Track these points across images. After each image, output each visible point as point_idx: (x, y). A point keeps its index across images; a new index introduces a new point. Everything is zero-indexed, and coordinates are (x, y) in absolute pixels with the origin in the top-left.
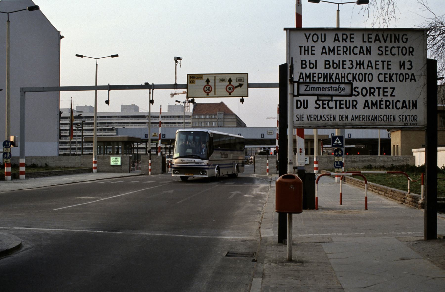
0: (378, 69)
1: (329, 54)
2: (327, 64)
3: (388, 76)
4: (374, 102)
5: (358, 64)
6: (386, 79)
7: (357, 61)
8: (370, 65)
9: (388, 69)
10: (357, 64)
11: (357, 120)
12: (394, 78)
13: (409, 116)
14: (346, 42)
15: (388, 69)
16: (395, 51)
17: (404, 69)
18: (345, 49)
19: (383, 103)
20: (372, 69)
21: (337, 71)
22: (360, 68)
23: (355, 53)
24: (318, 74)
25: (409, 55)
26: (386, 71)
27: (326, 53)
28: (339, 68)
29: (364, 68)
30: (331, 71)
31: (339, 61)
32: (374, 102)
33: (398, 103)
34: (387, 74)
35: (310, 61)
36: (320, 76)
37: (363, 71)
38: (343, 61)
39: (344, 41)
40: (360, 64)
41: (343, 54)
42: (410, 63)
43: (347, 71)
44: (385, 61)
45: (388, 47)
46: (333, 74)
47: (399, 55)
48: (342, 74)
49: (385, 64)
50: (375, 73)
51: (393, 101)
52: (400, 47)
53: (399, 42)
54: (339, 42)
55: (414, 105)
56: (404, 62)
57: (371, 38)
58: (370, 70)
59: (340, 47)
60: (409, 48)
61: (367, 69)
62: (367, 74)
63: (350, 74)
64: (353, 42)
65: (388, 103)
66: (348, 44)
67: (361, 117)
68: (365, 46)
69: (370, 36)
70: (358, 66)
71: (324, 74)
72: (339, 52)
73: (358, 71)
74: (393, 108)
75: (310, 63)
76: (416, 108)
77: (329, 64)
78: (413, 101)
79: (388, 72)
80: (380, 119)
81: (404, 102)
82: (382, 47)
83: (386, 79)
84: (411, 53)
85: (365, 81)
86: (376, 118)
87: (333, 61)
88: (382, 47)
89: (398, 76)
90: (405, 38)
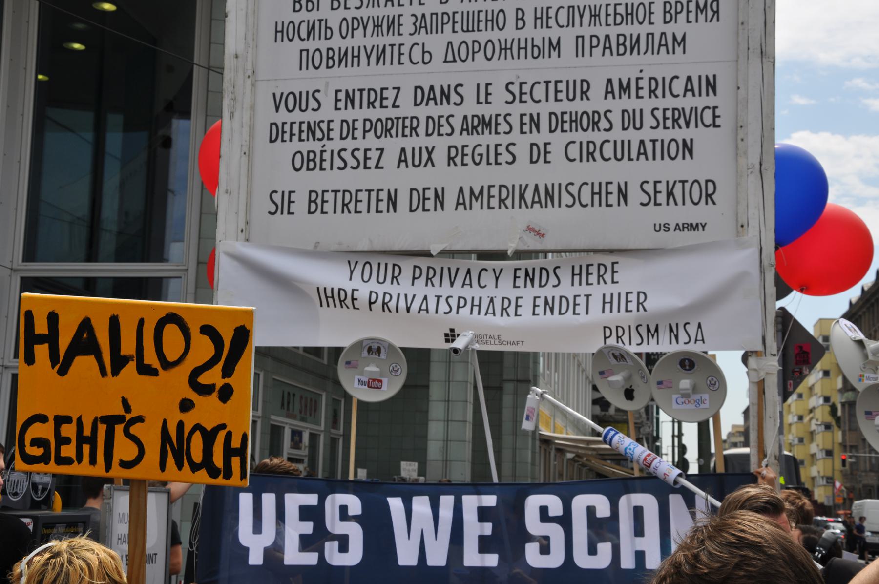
11: (476, 205)
13: (683, 182)
67: (494, 191)
80: (567, 199)
86: (549, 195)
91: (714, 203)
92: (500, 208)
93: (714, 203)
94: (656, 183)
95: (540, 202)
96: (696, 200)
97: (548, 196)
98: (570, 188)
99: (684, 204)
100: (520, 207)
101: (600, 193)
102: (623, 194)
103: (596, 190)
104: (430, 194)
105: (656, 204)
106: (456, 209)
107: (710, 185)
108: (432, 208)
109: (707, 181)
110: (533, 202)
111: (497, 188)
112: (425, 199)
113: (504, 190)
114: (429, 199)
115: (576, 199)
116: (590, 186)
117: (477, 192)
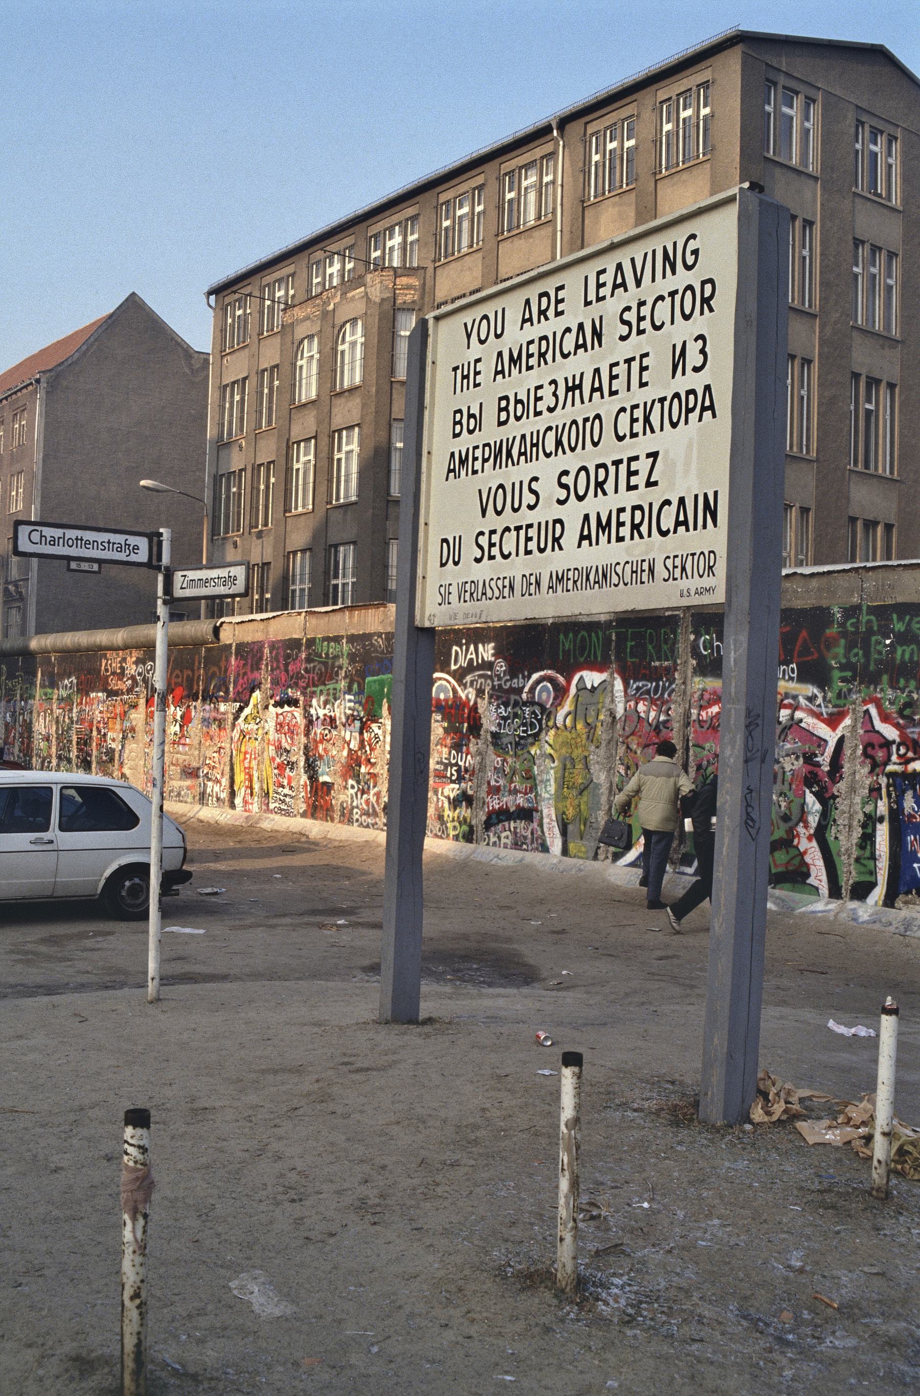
3: (639, 413)
10: (568, 389)
13: (693, 555)
16: (663, 311)
19: (626, 517)
29: (582, 402)
30: (514, 429)
44: (633, 359)
80: (615, 580)
86: (605, 576)
101: (636, 572)
102: (651, 571)
110: (595, 582)
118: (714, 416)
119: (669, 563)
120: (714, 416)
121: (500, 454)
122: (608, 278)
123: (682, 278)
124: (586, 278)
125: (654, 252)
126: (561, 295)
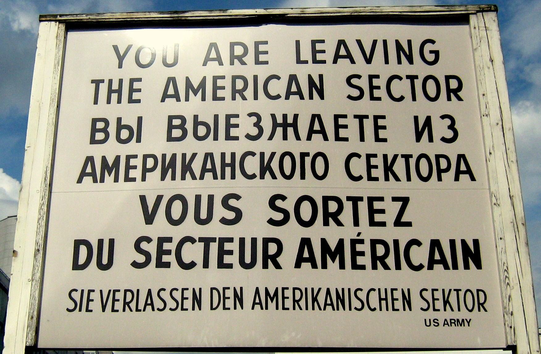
0: (346, 139)
1: (187, 99)
2: (176, 127)
3: (378, 161)
4: (333, 246)
5: (280, 125)
6: (374, 173)
7: (273, 116)
8: (317, 127)
9: (378, 139)
10: (275, 125)
11: (272, 305)
12: (399, 167)
13: (458, 291)
14: (243, 63)
15: (378, 139)
16: (401, 88)
17: (431, 140)
18: (240, 84)
19: (366, 248)
20: (326, 138)
21: (209, 146)
22: (285, 137)
23: (273, 93)
24: (145, 157)
25: (449, 99)
26: (370, 145)
27: (176, 96)
28: (216, 138)
30: (189, 146)
31: (216, 117)
32: (333, 246)
33: (414, 248)
34: (375, 156)
35: (119, 120)
36: (150, 163)
37: (296, 147)
38: (228, 117)
39: (236, 61)
40: (285, 125)
41: (234, 98)
42: (448, 122)
43: (241, 146)
44: (367, 117)
45: (377, 77)
46: (194, 155)
47: (414, 99)
48: (223, 155)
49: (369, 124)
50: (337, 152)
51: (396, 242)
52: (416, 77)
53: (411, 62)
54: (221, 64)
55: (473, 255)
56: (428, 119)
57: (323, 52)
58: (317, 144)
59: (223, 77)
60: (448, 78)
61: (309, 138)
62: (308, 154)
63: (253, 154)
64: (266, 63)
65: (380, 250)
66: (250, 70)
68: (302, 73)
69: (319, 47)
70: (279, 130)
71: (164, 156)
72: (220, 93)
73: (278, 145)
74: (398, 267)
75: (120, 126)
76: (479, 266)
77: (182, 127)
78: (463, 242)
79: (379, 149)
80: (356, 303)
81: (435, 244)
82: (359, 77)
83: (374, 173)
84: (454, 93)
85: (303, 177)
86: (340, 299)
87: (196, 117)
88: (359, 77)
89: (412, 162)
90: (431, 52)
91: (486, 311)
92: (294, 309)
93: (486, 311)
94: (433, 290)
95: (332, 304)
96: (470, 308)
97: (339, 300)
98: (359, 293)
99: (459, 310)
100: (313, 309)
101: (386, 299)
102: (407, 301)
103: (383, 296)
104: (230, 293)
105: (435, 310)
106: (253, 308)
107: (481, 294)
108: (232, 307)
109: (478, 291)
111: (291, 290)
112: (225, 298)
113: (298, 293)
114: (229, 298)
115: (365, 304)
116: (377, 291)
117: (272, 293)
118: (473, 179)
119: (428, 295)
120: (473, 179)
121: (168, 167)
122: (330, 48)
123: (420, 69)
124: (298, 43)
125: (385, 42)
126: (262, 48)
